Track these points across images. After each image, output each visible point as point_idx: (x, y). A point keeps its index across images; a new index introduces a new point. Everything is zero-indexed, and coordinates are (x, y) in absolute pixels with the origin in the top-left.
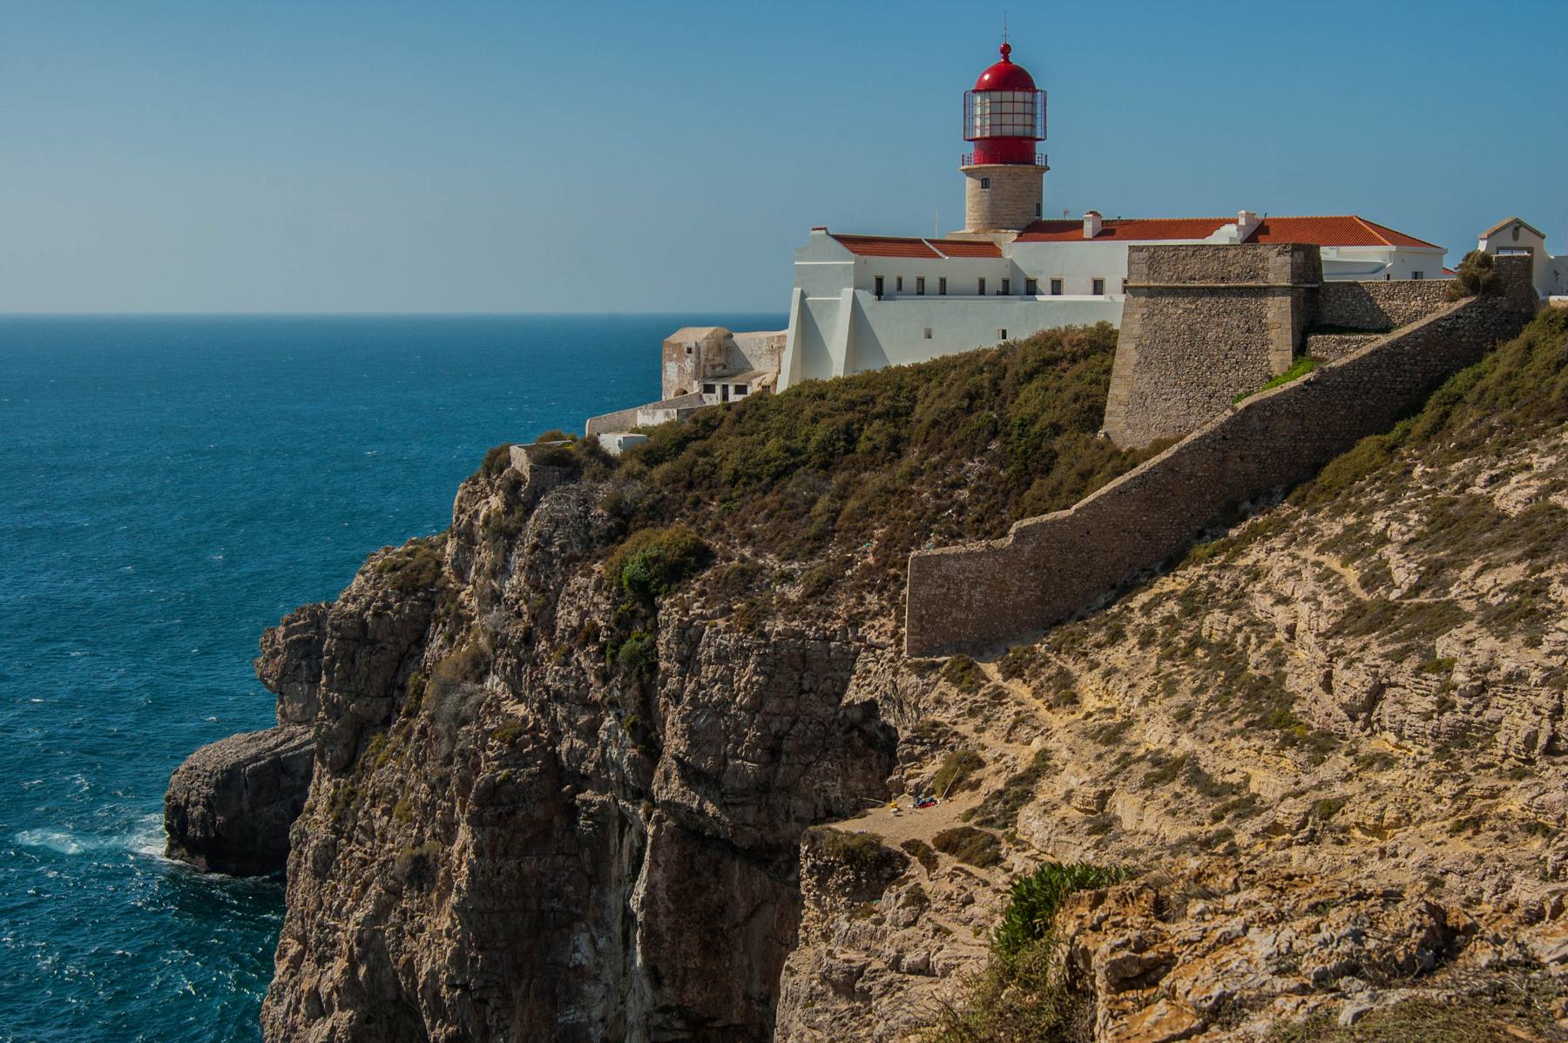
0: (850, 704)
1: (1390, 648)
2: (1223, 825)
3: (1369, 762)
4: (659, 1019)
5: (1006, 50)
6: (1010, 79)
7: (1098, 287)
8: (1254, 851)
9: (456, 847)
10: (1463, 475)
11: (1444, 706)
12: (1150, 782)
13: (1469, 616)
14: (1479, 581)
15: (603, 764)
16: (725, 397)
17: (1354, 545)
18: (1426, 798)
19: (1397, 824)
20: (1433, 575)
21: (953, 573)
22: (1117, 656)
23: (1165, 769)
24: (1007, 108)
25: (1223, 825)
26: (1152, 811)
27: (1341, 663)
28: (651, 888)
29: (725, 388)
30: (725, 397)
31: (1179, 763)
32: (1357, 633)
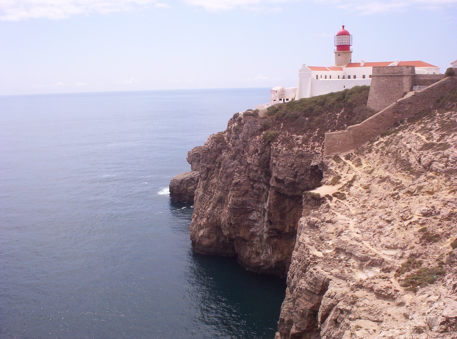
0: (312, 166)
1: (434, 153)
2: (396, 192)
3: (429, 178)
4: (271, 231)
5: (343, 27)
6: (344, 33)
7: (364, 77)
8: (404, 197)
9: (229, 195)
10: (448, 116)
11: (446, 166)
12: (379, 182)
13: (452, 146)
14: (454, 138)
16: (284, 101)
17: (424, 130)
18: (443, 186)
19: (436, 191)
20: (442, 136)
21: (335, 137)
22: (371, 155)
23: (383, 179)
24: (344, 39)
25: (396, 192)
26: (381, 188)
27: (423, 156)
28: (269, 204)
29: (284, 99)
30: (284, 101)
31: (386, 178)
32: (426, 149)
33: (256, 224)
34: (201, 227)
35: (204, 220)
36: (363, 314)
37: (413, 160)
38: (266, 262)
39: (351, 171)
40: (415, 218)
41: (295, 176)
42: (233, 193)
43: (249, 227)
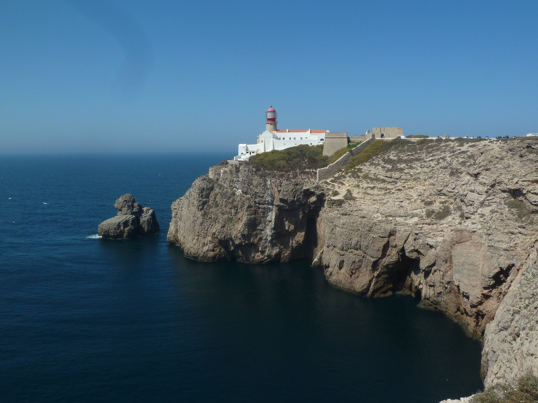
3: (405, 183)
7: (290, 139)
15: (266, 201)
25: (388, 191)
33: (263, 232)
35: (209, 238)
36: (430, 231)
37: (382, 177)
38: (269, 256)
39: (341, 188)
40: (415, 198)
41: (294, 197)
42: (248, 212)
43: (256, 235)
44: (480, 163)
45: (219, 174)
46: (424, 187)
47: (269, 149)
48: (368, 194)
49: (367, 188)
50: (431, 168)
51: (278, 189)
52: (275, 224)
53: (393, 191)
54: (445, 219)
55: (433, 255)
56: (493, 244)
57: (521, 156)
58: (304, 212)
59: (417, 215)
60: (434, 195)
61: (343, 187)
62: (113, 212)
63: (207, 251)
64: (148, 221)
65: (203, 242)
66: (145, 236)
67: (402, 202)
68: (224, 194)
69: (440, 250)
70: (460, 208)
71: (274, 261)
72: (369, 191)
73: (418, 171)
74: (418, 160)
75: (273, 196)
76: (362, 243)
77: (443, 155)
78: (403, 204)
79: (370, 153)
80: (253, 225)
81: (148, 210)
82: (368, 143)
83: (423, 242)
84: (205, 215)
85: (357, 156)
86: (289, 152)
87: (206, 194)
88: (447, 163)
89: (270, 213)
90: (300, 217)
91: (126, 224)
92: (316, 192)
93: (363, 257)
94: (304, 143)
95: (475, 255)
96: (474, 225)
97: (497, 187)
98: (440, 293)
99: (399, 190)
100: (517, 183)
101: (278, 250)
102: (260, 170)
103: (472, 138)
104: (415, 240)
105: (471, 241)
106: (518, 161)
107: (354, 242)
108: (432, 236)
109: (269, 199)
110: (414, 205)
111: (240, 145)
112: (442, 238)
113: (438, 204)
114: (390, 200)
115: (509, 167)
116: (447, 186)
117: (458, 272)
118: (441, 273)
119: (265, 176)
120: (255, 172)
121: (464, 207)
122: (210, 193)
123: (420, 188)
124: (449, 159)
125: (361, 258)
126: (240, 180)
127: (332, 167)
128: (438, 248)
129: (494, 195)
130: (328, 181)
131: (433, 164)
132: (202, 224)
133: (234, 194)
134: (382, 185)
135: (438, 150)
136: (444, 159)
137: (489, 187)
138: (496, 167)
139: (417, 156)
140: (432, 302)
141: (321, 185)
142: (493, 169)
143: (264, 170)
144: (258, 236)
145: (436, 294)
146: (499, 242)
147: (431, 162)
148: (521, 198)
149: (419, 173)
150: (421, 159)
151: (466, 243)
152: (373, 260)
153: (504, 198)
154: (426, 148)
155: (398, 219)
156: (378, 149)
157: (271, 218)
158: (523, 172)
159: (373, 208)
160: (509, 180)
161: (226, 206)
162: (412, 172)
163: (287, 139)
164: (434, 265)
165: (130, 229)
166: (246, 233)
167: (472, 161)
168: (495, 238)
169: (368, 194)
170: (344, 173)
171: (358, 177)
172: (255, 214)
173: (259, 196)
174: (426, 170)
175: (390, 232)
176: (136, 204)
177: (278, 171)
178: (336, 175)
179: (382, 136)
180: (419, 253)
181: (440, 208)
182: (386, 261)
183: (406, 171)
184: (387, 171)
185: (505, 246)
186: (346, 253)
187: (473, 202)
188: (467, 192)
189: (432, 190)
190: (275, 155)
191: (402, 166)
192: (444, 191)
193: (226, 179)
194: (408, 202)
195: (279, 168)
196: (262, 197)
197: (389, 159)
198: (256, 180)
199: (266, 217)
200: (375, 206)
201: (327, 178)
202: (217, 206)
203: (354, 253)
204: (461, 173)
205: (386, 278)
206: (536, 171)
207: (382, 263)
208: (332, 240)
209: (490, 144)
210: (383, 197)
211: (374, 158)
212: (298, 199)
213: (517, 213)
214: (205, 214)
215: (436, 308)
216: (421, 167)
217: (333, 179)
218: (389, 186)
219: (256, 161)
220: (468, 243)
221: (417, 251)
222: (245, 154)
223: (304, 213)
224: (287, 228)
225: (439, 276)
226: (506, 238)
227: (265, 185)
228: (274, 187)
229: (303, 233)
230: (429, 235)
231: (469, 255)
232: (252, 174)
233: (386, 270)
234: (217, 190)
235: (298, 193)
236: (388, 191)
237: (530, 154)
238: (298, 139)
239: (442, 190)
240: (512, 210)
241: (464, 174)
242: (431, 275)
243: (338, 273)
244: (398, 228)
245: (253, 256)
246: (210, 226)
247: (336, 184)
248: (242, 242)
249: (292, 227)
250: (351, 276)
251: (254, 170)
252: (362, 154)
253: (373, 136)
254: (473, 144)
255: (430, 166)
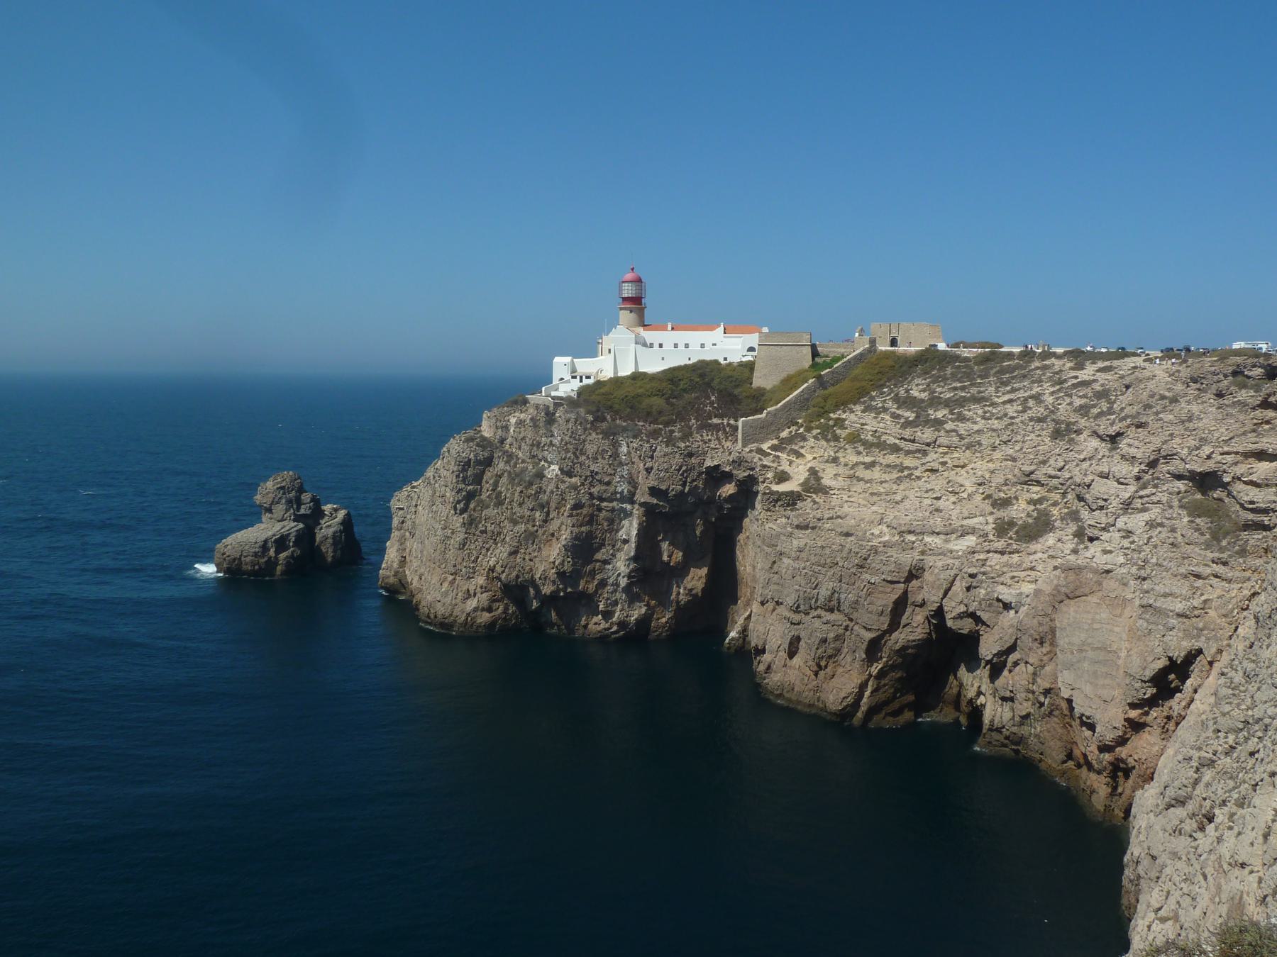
3: (946, 453)
7: (676, 346)
15: (616, 493)
22: (811, 442)
25: (906, 473)
27: (919, 434)
33: (608, 567)
34: (468, 595)
35: (481, 580)
36: (1005, 570)
37: (891, 440)
38: (622, 624)
39: (794, 465)
40: (970, 490)
41: (684, 485)
43: (593, 574)
44: (1122, 409)
45: (506, 428)
46: (991, 466)
47: (626, 370)
48: (859, 479)
49: (857, 464)
50: (1007, 421)
51: (645, 464)
52: (637, 548)
53: (917, 473)
54: (1041, 540)
55: (1012, 626)
56: (1151, 601)
57: (1220, 395)
58: (705, 520)
59: (972, 531)
60: (1014, 484)
61: (799, 461)
62: (252, 515)
63: (476, 609)
64: (334, 537)
65: (465, 588)
66: (326, 574)
67: (938, 498)
68: (517, 475)
69: (1027, 615)
70: (1074, 516)
71: (636, 636)
72: (861, 472)
73: (976, 427)
74: (977, 400)
75: (633, 483)
76: (843, 596)
77: (1036, 389)
78: (941, 504)
79: (864, 383)
80: (585, 549)
81: (336, 510)
82: (860, 358)
83: (987, 594)
84: (471, 524)
85: (836, 388)
86: (672, 376)
87: (473, 471)
88: (1046, 408)
89: (626, 523)
90: (698, 533)
91: (281, 543)
92: (735, 472)
93: (846, 629)
94: (708, 358)
95: (1109, 627)
96: (1109, 556)
97: (1163, 467)
98: (1027, 716)
99: (932, 471)
100: (1209, 457)
101: (643, 610)
102: (604, 419)
103: (1104, 350)
104: (968, 589)
105: (1100, 594)
106: (1211, 405)
107: (824, 593)
108: (1010, 582)
109: (624, 488)
110: (967, 508)
111: (557, 360)
112: (1033, 586)
113: (1023, 505)
114: (911, 494)
115: (1190, 420)
116: (1044, 462)
117: (1069, 666)
118: (1030, 669)
119: (614, 434)
120: (592, 423)
121: (1085, 514)
122: (483, 472)
123: (982, 467)
124: (1050, 400)
125: (841, 631)
126: (556, 441)
127: (775, 414)
128: (1023, 609)
129: (1156, 486)
130: (765, 446)
131: (1011, 410)
132: (462, 546)
133: (540, 475)
134: (892, 459)
135: (1024, 376)
136: (1037, 398)
137: (1143, 467)
138: (1161, 419)
139: (974, 390)
140: (1007, 738)
141: (749, 457)
142: (1154, 425)
143: (614, 420)
144: (598, 577)
145: (1017, 719)
146: (1165, 595)
147: (1008, 406)
148: (1217, 494)
149: (978, 431)
150: (984, 399)
151: (1089, 598)
152: (869, 636)
153: (1179, 493)
154: (998, 372)
155: (928, 539)
156: (883, 372)
157: (628, 535)
158: (1223, 432)
159: (868, 512)
160: (1191, 450)
161: (521, 505)
162: (963, 428)
163: (668, 346)
164: (1012, 649)
165: (292, 556)
166: (567, 567)
167: (1104, 405)
168: (1157, 588)
169: (859, 479)
170: (802, 430)
171: (836, 438)
172: (590, 523)
173: (600, 482)
174: (996, 424)
175: (910, 571)
176: (306, 497)
177: (645, 421)
178: (784, 434)
179: (894, 342)
180: (978, 620)
181: (1029, 515)
182: (900, 638)
183: (949, 426)
184: (904, 426)
185: (1179, 606)
186: (808, 618)
187: (1106, 500)
188: (1091, 478)
189: (1010, 472)
190: (639, 384)
191: (939, 414)
192: (1039, 475)
193: (523, 438)
194: (953, 499)
195: (649, 416)
196: (608, 483)
197: (908, 397)
198: (594, 442)
199: (617, 531)
200: (874, 508)
201: (763, 441)
202: (500, 503)
203: (824, 620)
204: (1078, 432)
205: (900, 679)
206: (1254, 431)
207: (890, 643)
208: (773, 587)
209: (1147, 364)
210: (895, 487)
211: (874, 394)
212: (693, 490)
213: (1209, 528)
214: (470, 524)
215: (1017, 752)
216: (984, 418)
217: (776, 442)
218: (908, 462)
219: (594, 397)
220: (1093, 599)
221: (973, 615)
222: (568, 382)
223: (706, 522)
224: (665, 558)
225: (1025, 676)
226: (1183, 587)
227: (616, 455)
228: (636, 460)
229: (704, 571)
230: (1002, 579)
231: (1095, 626)
232: (585, 429)
233: (900, 660)
234: (501, 465)
235: (694, 474)
236: (906, 473)
237: (1240, 389)
238: (695, 346)
239: (1032, 473)
240: (1198, 520)
241: (1085, 434)
242: (1006, 672)
243: (785, 666)
244: (929, 560)
245: (583, 623)
246: (484, 551)
247: (783, 456)
248: (558, 590)
249: (678, 556)
250: (816, 674)
251: (590, 418)
252: (845, 385)
253: (873, 342)
254: (1108, 363)
255: (1006, 415)
